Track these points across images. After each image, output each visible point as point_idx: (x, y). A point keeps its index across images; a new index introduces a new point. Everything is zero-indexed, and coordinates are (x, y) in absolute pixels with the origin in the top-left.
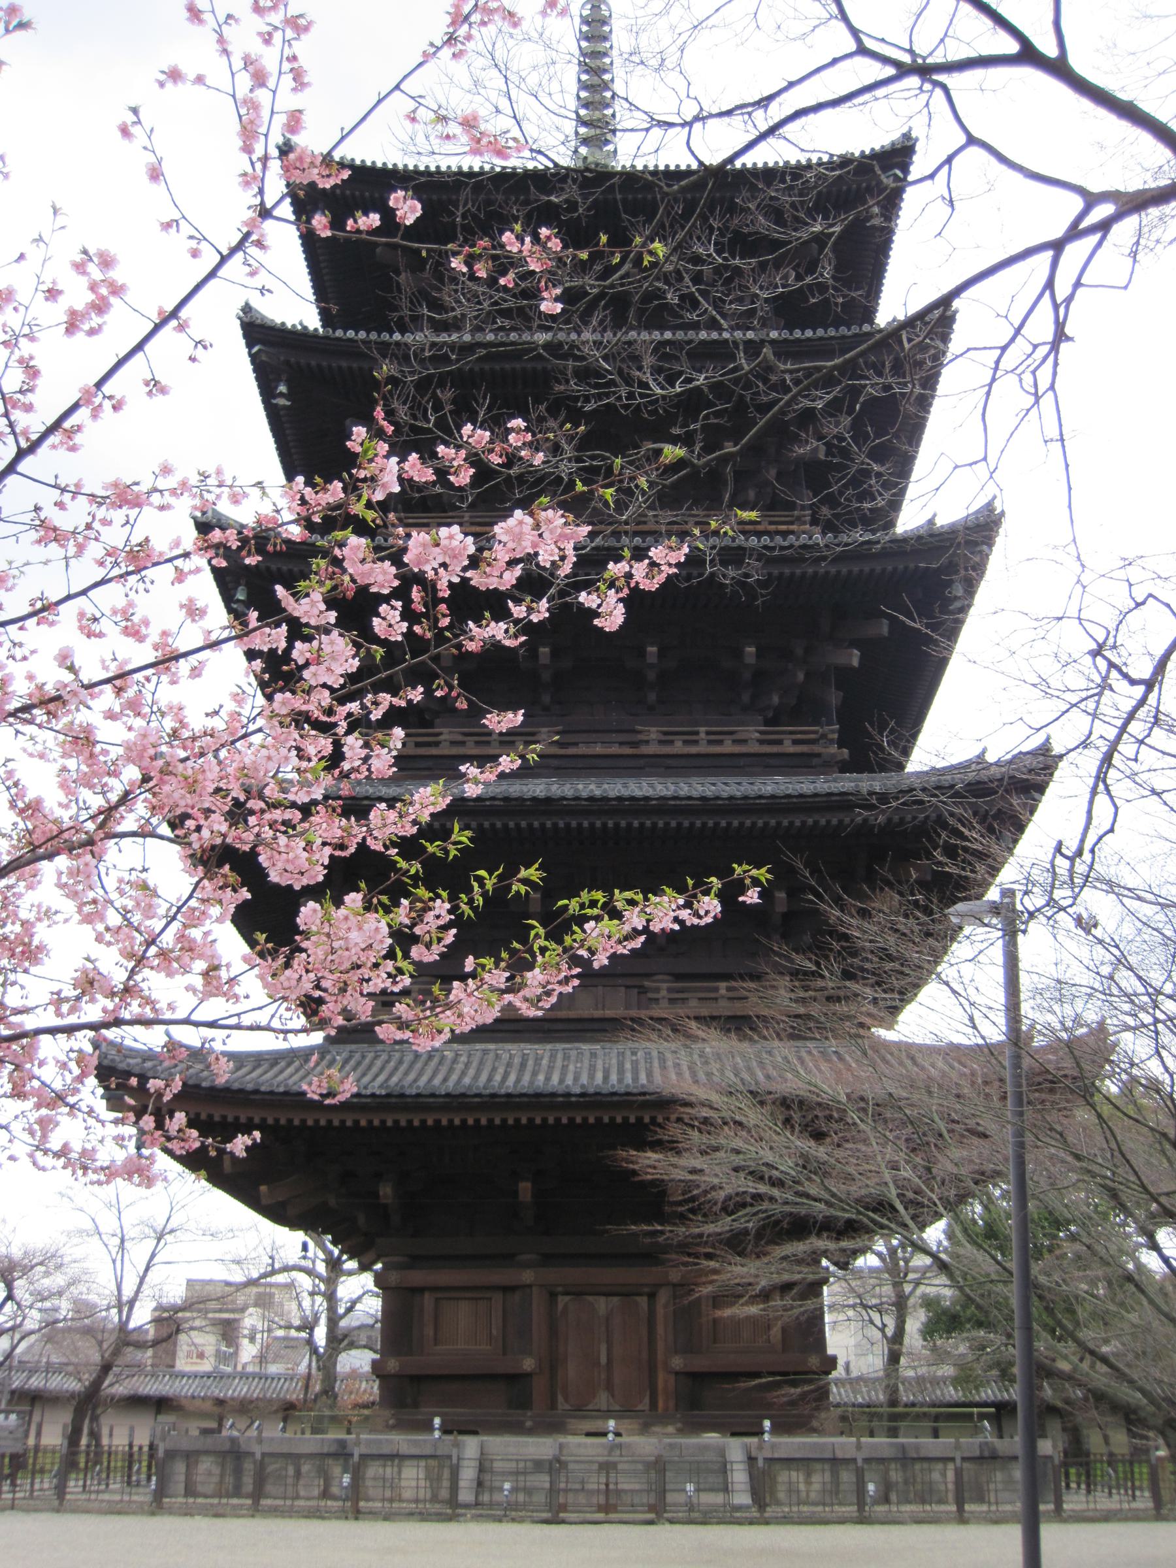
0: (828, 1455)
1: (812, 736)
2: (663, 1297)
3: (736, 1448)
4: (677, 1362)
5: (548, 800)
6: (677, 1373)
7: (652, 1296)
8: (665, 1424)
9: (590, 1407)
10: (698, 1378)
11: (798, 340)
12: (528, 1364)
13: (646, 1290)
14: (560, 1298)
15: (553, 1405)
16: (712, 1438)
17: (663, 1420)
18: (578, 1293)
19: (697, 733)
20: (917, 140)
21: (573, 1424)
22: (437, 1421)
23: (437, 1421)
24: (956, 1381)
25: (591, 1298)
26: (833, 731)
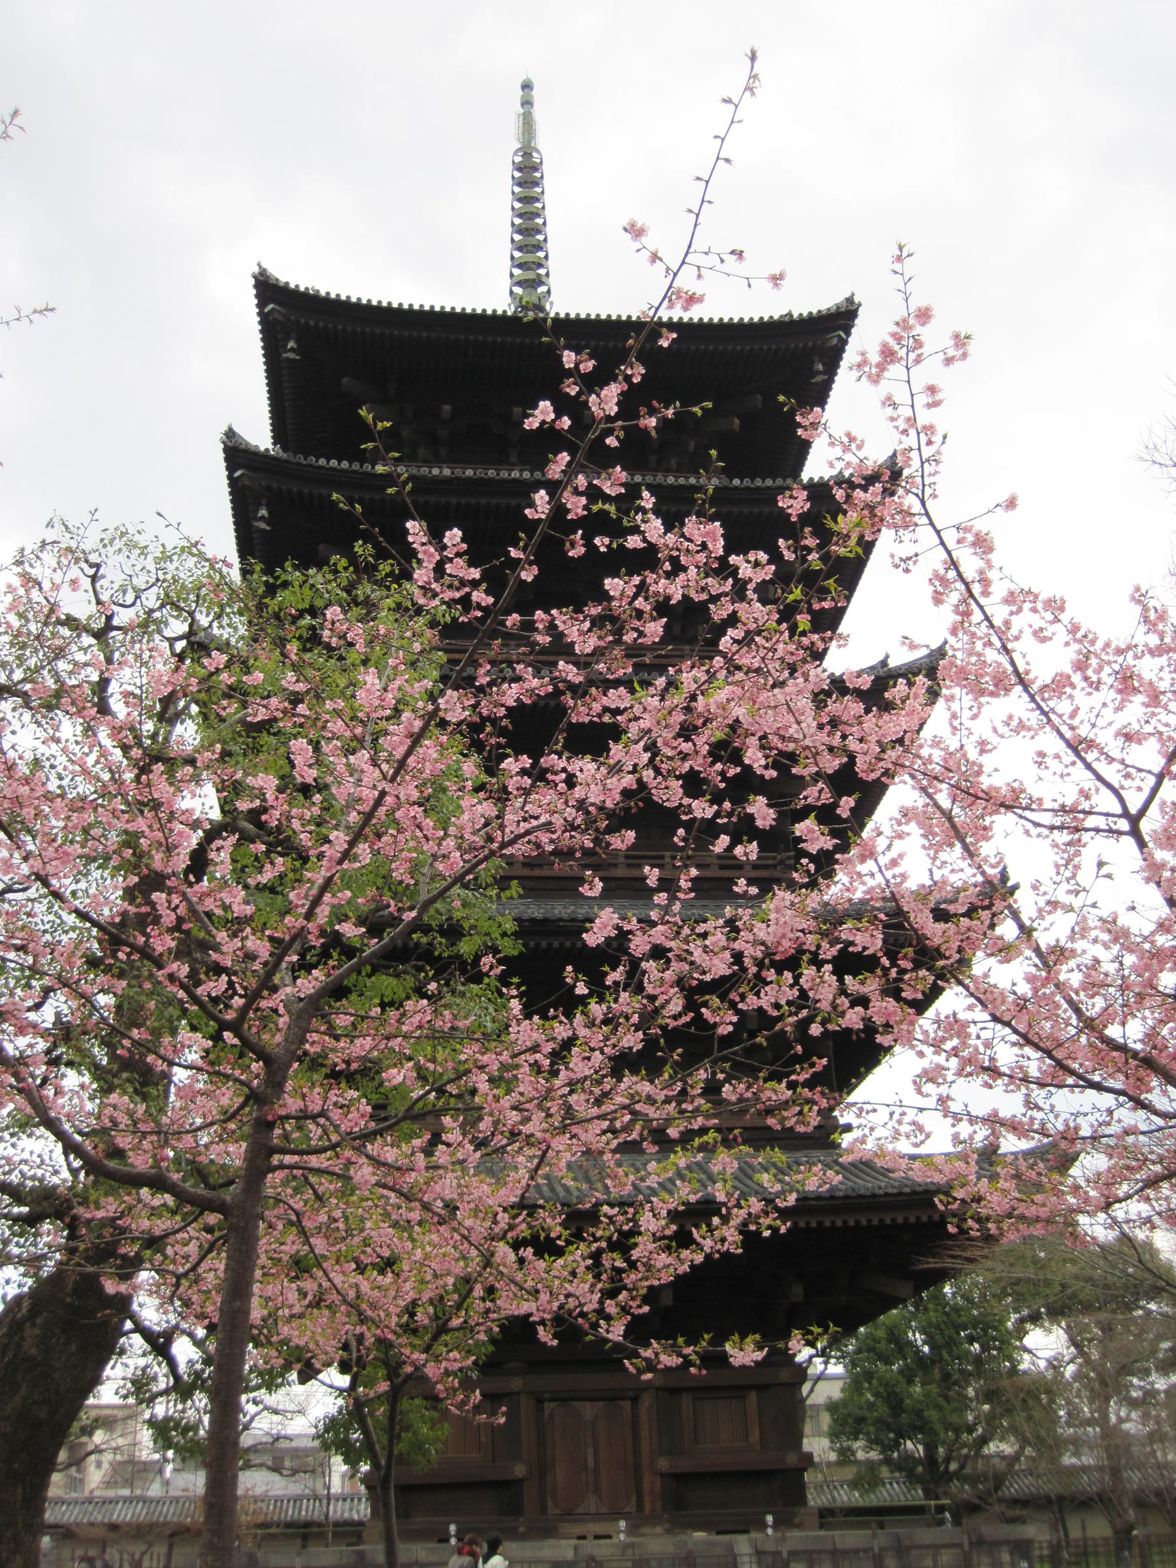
0: (829, 1547)
1: (770, 862)
2: (646, 1401)
3: (743, 1544)
4: (663, 1464)
5: (545, 921)
6: (662, 1475)
7: (635, 1400)
8: (654, 1525)
9: (580, 1510)
10: (682, 1479)
11: (758, 489)
12: (519, 1470)
13: (630, 1394)
14: (546, 1404)
15: (543, 1510)
16: (700, 1535)
17: (653, 1520)
18: (564, 1399)
19: (662, 857)
20: (860, 305)
21: (566, 1528)
22: (453, 1528)
23: (453, 1528)
24: (854, 1484)
25: (576, 1404)
26: (789, 858)
